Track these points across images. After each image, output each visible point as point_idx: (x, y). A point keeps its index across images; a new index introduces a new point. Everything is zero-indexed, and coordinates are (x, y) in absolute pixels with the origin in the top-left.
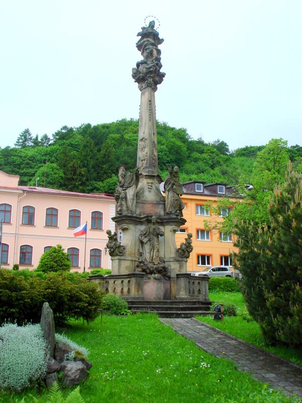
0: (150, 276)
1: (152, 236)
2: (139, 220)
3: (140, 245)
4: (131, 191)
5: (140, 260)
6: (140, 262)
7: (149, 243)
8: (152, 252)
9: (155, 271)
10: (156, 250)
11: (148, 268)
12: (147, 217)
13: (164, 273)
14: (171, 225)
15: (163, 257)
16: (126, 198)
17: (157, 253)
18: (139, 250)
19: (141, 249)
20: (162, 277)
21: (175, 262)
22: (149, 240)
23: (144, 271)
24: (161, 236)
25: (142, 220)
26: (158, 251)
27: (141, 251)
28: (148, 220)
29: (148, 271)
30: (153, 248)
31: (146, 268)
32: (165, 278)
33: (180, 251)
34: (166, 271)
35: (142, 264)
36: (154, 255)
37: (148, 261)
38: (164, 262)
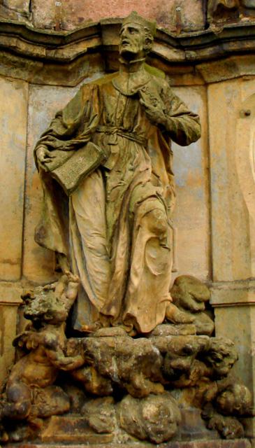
0: (102, 413)
1: (119, 143)
2: (40, 51)
3: (51, 207)
5: (34, 308)
6: (40, 322)
7: (96, 185)
8: (121, 250)
9: (139, 380)
10: (144, 236)
11: (89, 360)
12: (98, 30)
13: (211, 390)
15: (202, 274)
17: (153, 253)
18: (40, 236)
19: (55, 230)
20: (195, 420)
22: (101, 169)
23: (63, 379)
24: (183, 140)
25: (68, 53)
26: (159, 237)
27: (54, 241)
28: (105, 49)
30: (126, 218)
31: (78, 359)
32: (217, 418)
34: (215, 376)
35: (51, 335)
36: (137, 265)
37: (99, 304)
38: (210, 309)
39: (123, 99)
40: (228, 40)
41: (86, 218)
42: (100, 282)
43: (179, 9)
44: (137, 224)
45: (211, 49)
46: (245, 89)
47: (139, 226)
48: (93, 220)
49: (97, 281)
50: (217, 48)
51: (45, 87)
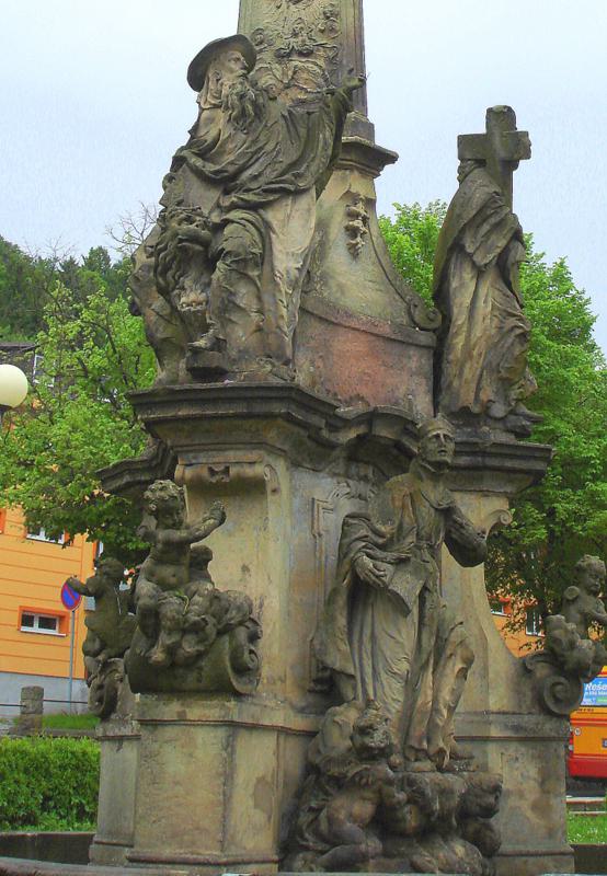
4: (295, 224)
14: (486, 494)
16: (263, 258)
21: (513, 748)
27: (337, 660)
29: (411, 818)
33: (542, 671)
35: (384, 769)
39: (432, 510)
40: (490, 455)
41: (401, 640)
42: (394, 711)
43: (410, 397)
44: (448, 652)
45: (468, 458)
46: (484, 505)
47: (451, 655)
48: (406, 643)
49: (391, 709)
50: (473, 458)
51: (301, 469)
